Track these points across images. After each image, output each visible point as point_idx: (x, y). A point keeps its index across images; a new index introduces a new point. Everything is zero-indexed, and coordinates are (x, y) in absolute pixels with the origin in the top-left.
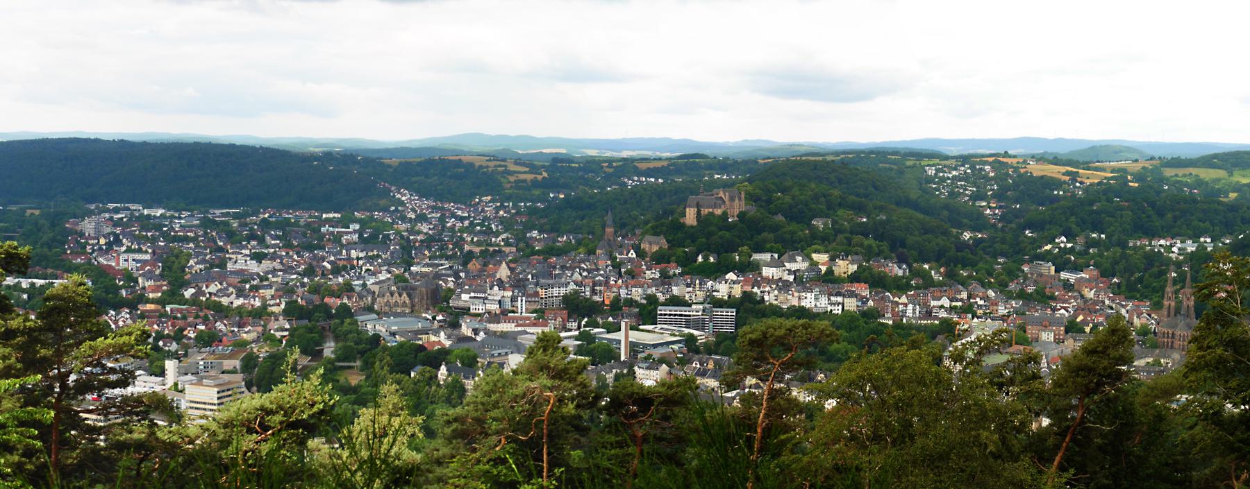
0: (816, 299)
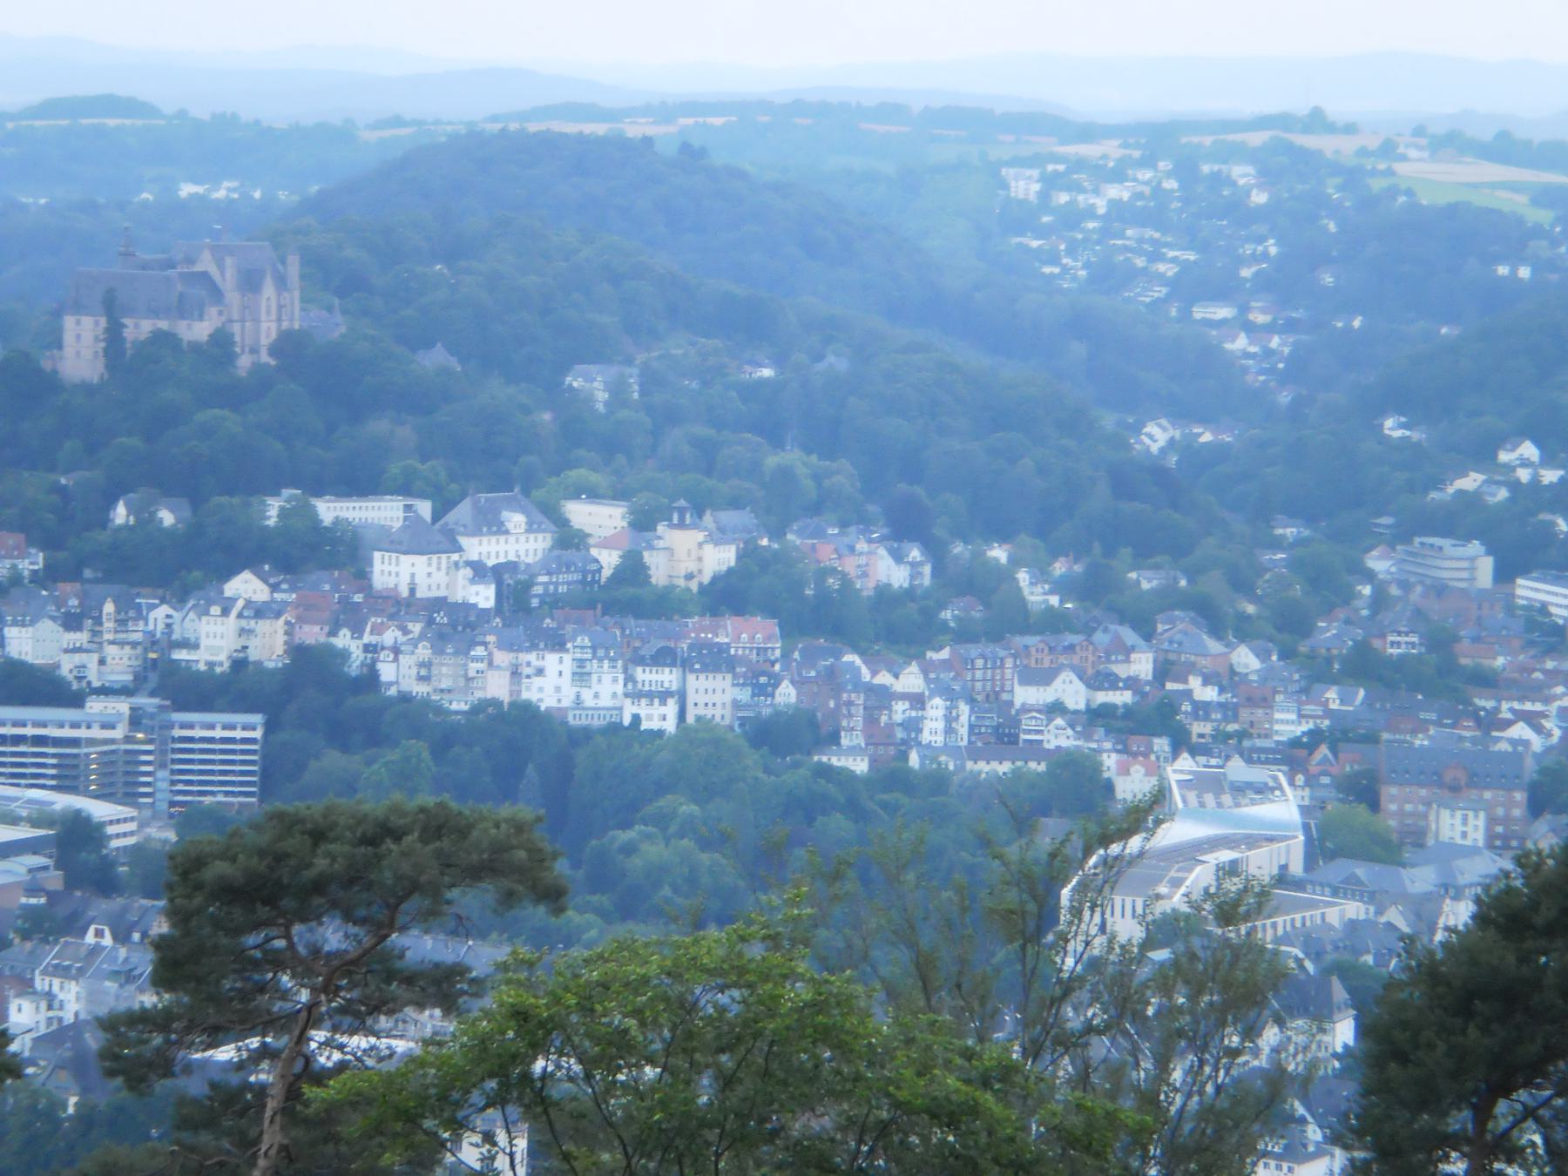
0: (581, 676)
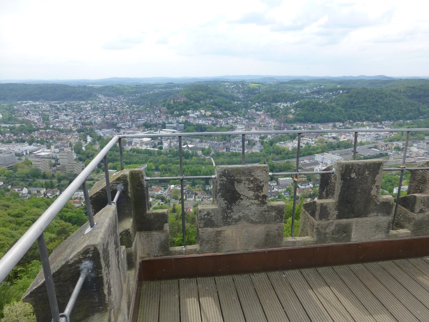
0: (202, 121)
